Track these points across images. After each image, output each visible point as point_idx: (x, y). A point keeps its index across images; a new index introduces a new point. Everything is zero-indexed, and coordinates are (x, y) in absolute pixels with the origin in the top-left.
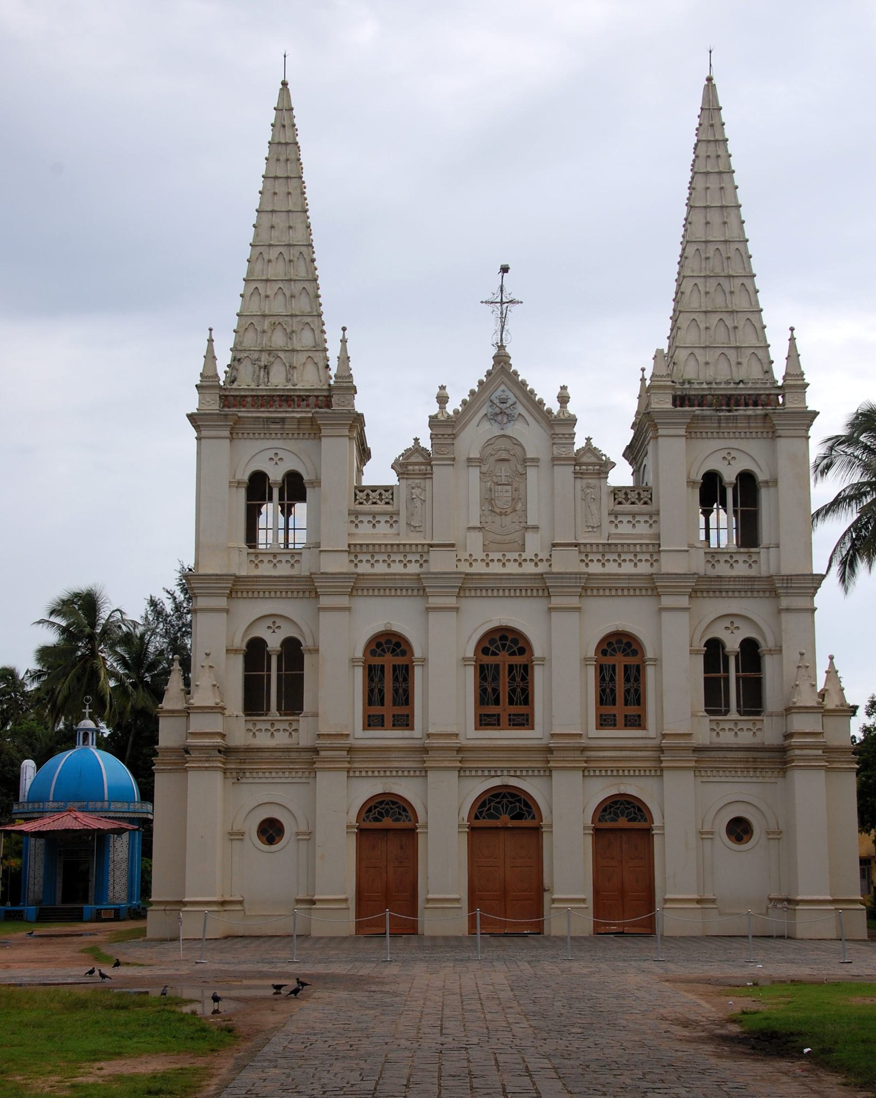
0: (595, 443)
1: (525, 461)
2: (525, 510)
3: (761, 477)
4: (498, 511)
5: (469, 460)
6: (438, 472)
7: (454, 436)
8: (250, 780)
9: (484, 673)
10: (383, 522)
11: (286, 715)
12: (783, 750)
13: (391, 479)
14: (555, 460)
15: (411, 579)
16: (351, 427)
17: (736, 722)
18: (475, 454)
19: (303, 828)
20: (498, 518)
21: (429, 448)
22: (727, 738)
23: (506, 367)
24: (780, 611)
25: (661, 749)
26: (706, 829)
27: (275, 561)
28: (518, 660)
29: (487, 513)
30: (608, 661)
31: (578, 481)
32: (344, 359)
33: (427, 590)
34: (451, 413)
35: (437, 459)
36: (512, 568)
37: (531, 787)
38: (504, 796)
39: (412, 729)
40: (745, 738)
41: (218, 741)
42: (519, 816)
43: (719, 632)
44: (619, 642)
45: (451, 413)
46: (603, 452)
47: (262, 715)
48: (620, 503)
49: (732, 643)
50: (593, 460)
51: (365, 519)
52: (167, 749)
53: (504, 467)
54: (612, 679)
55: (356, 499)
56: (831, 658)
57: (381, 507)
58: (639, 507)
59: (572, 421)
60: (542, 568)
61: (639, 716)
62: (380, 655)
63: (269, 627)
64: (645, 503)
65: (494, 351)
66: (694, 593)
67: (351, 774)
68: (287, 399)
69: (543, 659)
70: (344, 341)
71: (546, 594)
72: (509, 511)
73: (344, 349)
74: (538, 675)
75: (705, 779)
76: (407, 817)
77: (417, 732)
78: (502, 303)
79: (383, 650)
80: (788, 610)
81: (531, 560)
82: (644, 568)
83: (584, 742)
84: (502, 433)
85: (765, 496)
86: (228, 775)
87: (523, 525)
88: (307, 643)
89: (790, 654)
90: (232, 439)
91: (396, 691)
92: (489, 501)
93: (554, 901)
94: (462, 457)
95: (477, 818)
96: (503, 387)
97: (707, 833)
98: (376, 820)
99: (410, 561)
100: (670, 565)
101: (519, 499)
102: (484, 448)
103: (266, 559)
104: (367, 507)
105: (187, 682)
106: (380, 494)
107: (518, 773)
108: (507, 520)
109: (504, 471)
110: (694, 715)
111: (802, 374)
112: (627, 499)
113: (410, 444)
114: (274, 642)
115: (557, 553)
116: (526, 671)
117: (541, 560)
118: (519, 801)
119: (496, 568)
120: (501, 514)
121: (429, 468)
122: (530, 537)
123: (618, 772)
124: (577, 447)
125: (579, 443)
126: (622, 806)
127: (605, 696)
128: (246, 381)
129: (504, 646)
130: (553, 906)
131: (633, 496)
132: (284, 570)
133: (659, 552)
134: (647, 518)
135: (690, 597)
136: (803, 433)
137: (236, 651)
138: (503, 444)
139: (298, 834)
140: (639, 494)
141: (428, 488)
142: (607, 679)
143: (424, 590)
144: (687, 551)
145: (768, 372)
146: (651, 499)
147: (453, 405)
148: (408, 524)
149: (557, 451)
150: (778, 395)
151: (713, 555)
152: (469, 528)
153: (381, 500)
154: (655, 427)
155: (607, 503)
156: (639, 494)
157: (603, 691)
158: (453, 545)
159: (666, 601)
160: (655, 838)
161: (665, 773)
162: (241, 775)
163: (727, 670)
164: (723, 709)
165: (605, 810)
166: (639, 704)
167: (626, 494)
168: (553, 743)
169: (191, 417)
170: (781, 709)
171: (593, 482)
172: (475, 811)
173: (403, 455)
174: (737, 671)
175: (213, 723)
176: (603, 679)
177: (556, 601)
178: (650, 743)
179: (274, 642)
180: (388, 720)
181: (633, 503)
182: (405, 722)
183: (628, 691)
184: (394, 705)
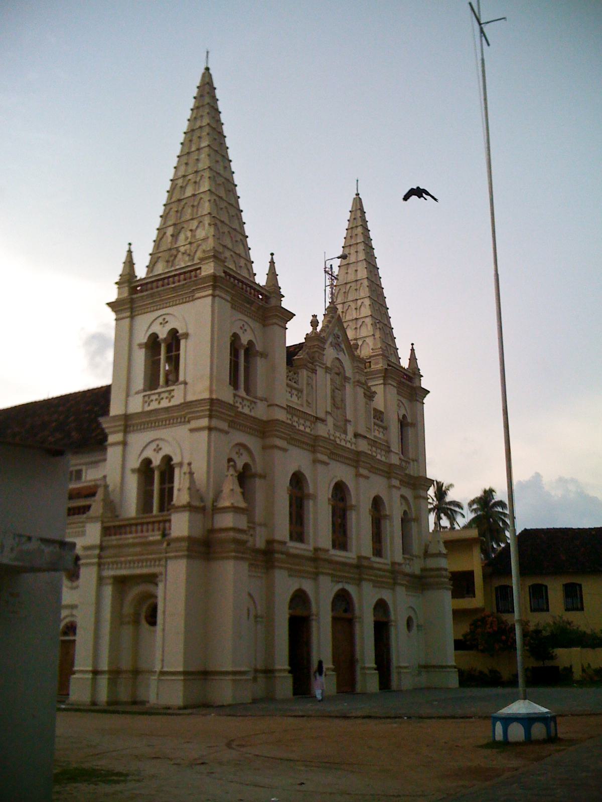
1: (346, 379)
36: (343, 443)
42: (346, 611)
60: (353, 447)
101: (343, 401)
141: (314, 378)
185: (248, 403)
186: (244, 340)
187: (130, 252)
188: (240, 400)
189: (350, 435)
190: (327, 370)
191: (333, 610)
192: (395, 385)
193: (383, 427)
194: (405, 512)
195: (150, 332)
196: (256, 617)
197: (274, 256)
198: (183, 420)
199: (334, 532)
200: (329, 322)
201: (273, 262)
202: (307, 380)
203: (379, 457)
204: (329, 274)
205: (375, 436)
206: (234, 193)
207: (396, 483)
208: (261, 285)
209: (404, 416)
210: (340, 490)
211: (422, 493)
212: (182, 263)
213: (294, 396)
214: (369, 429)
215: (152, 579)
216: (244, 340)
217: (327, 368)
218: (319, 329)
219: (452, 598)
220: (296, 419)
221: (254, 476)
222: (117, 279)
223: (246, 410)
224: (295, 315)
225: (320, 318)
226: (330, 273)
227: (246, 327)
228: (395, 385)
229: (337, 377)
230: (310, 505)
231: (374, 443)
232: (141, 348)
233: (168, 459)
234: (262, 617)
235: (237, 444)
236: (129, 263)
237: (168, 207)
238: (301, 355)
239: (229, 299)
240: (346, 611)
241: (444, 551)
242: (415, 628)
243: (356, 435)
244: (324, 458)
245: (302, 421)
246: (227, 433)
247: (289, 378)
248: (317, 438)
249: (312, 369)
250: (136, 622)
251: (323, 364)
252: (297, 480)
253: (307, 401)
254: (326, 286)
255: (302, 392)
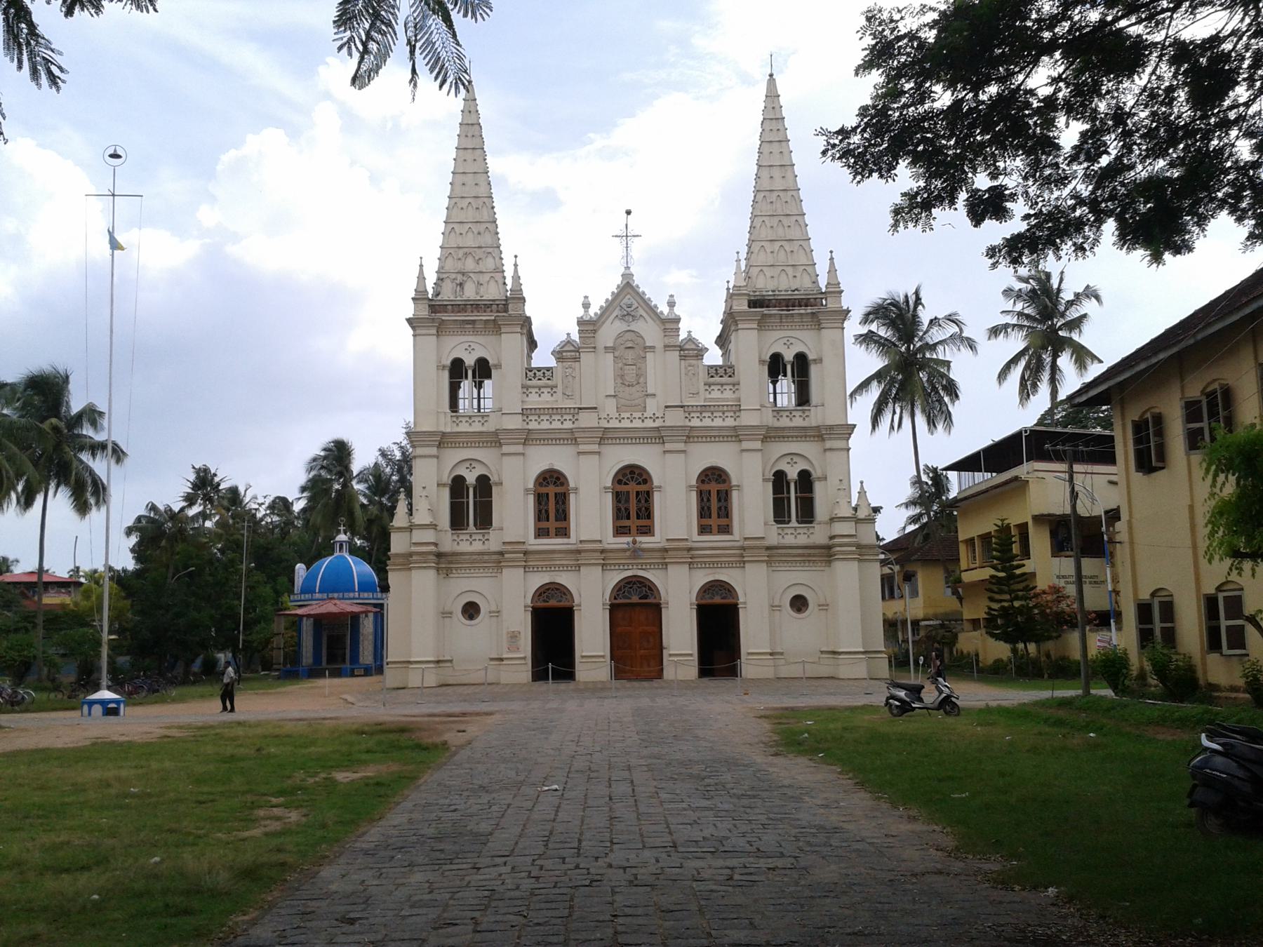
0: (693, 335)
1: (646, 349)
2: (646, 383)
3: (811, 356)
5: (606, 348)
6: (584, 357)
7: (595, 331)
8: (457, 575)
9: (618, 497)
10: (546, 393)
11: (480, 529)
12: (829, 547)
13: (551, 362)
14: (667, 347)
16: (522, 326)
17: (795, 528)
18: (610, 344)
19: (494, 608)
20: (627, 388)
21: (578, 340)
22: (789, 540)
23: (631, 282)
24: (825, 450)
25: (743, 548)
26: (776, 603)
27: (470, 421)
28: (643, 488)
29: (619, 385)
30: (706, 487)
31: (683, 361)
32: (516, 278)
33: (578, 440)
34: (593, 315)
35: (584, 348)
36: (637, 424)
37: (651, 575)
38: (634, 583)
39: (569, 537)
40: (802, 540)
41: (432, 548)
42: (646, 597)
43: (783, 466)
44: (713, 474)
45: (593, 315)
46: (700, 341)
47: (463, 529)
48: (712, 377)
49: (793, 474)
50: (693, 347)
51: (534, 391)
52: (397, 555)
53: (631, 351)
54: (709, 500)
55: (526, 377)
56: (862, 483)
57: (544, 381)
58: (725, 379)
59: (678, 320)
60: (658, 423)
61: (728, 526)
62: (546, 486)
63: (467, 468)
64: (730, 376)
65: (622, 270)
66: (765, 439)
67: (527, 570)
68: (477, 306)
69: (660, 487)
70: (516, 265)
71: (661, 441)
72: (634, 383)
73: (516, 271)
74: (657, 497)
75: (774, 569)
77: (573, 539)
78: (627, 236)
79: (548, 483)
80: (830, 449)
81: (651, 418)
82: (730, 422)
83: (689, 544)
84: (629, 328)
85: (814, 371)
86: (440, 572)
87: (644, 393)
88: (494, 479)
89: (833, 480)
90: (438, 336)
91: (557, 511)
92: (620, 377)
93: (670, 655)
94: (600, 345)
95: (615, 598)
96: (628, 296)
97: (776, 606)
98: (544, 601)
99: (565, 420)
100: (748, 419)
101: (641, 375)
102: (616, 339)
103: (464, 420)
104: (535, 382)
105: (410, 506)
106: (544, 373)
107: (644, 567)
108: (634, 389)
109: (630, 355)
110: (766, 524)
111: (839, 283)
112: (717, 374)
113: (564, 337)
114: (471, 478)
115: (669, 412)
116: (648, 495)
117: (658, 418)
118: (645, 586)
119: (625, 424)
120: (629, 386)
121: (577, 354)
122: (649, 401)
123: (714, 564)
124: (681, 338)
125: (683, 335)
126: (626, 589)
127: (704, 512)
128: (448, 294)
129: (632, 478)
130: (671, 659)
131: (721, 371)
132: (477, 427)
133: (740, 410)
134: (731, 387)
135: (762, 441)
136: (840, 325)
137: (444, 485)
138: (628, 336)
139: (490, 612)
140: (725, 370)
141: (577, 369)
142: (705, 500)
143: (576, 440)
144: (759, 410)
145: (815, 282)
146: (734, 373)
147: (594, 310)
148: (564, 394)
149: (667, 341)
150: (822, 298)
151: (778, 412)
152: (607, 396)
153: (544, 377)
154: (736, 323)
155: (703, 376)
156: (725, 370)
157: (703, 508)
158: (595, 408)
159: (745, 445)
160: (740, 610)
161: (747, 565)
162: (449, 571)
163: (789, 492)
164: (786, 519)
165: (705, 592)
166: (565, 520)
167: (716, 370)
168: (667, 545)
169: (409, 320)
170: (827, 518)
171: (693, 362)
172: (615, 593)
173: (559, 345)
174: (796, 493)
175: (429, 536)
176: (702, 500)
177: (668, 446)
178: (573, 547)
179: (471, 478)
180: (552, 531)
181: (721, 377)
182: (564, 532)
183: (720, 508)
184: (556, 520)
205: (705, 400)
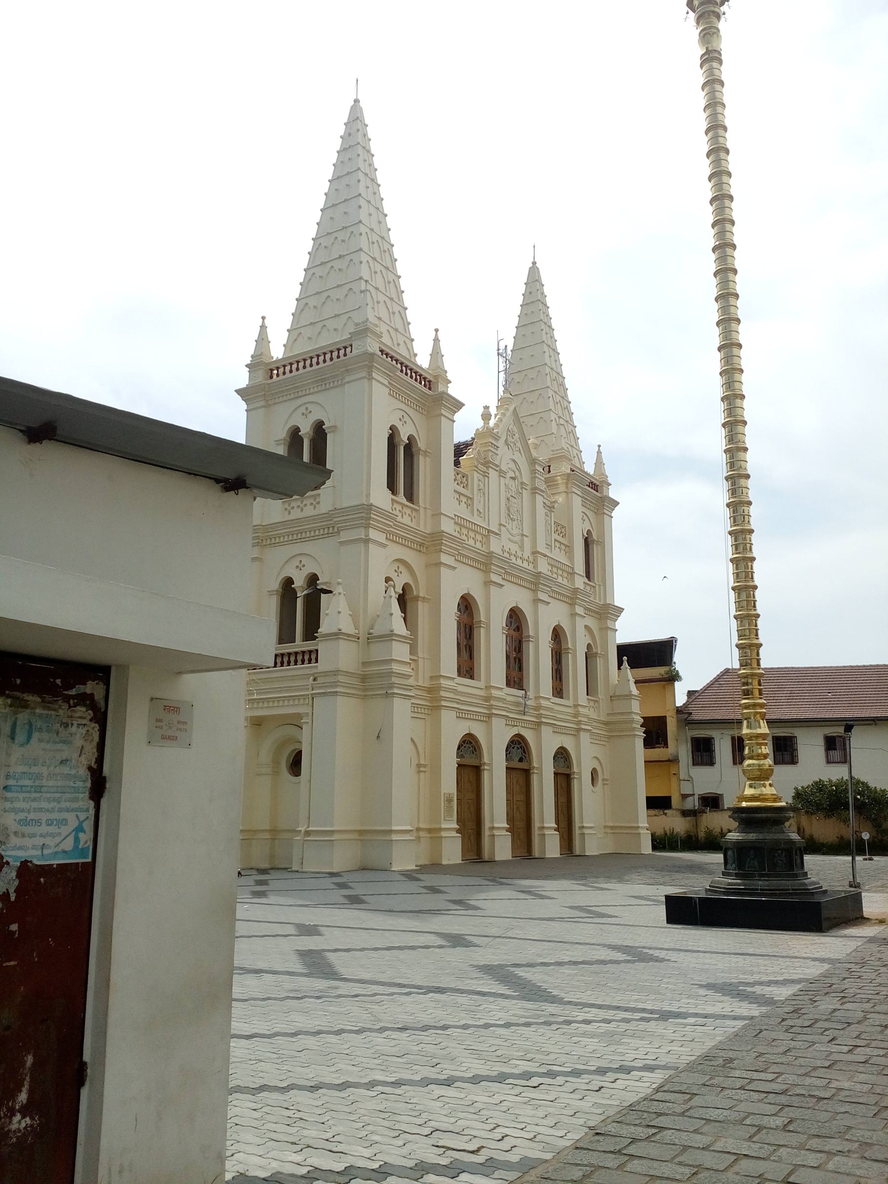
4: (511, 516)
15: (484, 555)
32: (436, 354)
36: (519, 562)
42: (521, 760)
60: (531, 567)
76: (476, 755)
185: (408, 511)
186: (404, 435)
187: (263, 327)
188: (399, 507)
189: (527, 553)
190: (502, 474)
191: (507, 760)
192: (579, 493)
193: (566, 546)
194: (589, 646)
195: (289, 425)
196: (419, 765)
197: (438, 333)
198: (331, 531)
199: (508, 667)
200: (504, 414)
201: (438, 339)
202: (479, 485)
203: (560, 580)
204: (504, 357)
206: (391, 255)
207: (579, 610)
208: (424, 368)
209: (589, 532)
210: (515, 618)
211: (610, 624)
212: (326, 340)
213: (463, 504)
214: (549, 545)
215: (295, 721)
216: (404, 435)
217: (501, 471)
218: (492, 423)
219: (645, 745)
220: (465, 531)
221: (417, 598)
222: (248, 360)
223: (406, 520)
224: (463, 405)
225: (493, 411)
226: (504, 355)
227: (406, 418)
228: (579, 493)
229: (512, 482)
230: (481, 635)
231: (554, 564)
232: (278, 445)
233: (313, 579)
234: (425, 766)
235: (396, 560)
236: (262, 340)
237: (311, 272)
238: (471, 454)
239: (386, 383)
240: (521, 760)
241: (634, 690)
242: (600, 782)
243: (535, 553)
244: (500, 581)
245: (472, 534)
246: (385, 546)
247: (456, 482)
248: (490, 555)
249: (485, 472)
250: (276, 773)
251: (497, 466)
252: (466, 605)
253: (478, 510)
254: (499, 372)
255: (472, 499)
